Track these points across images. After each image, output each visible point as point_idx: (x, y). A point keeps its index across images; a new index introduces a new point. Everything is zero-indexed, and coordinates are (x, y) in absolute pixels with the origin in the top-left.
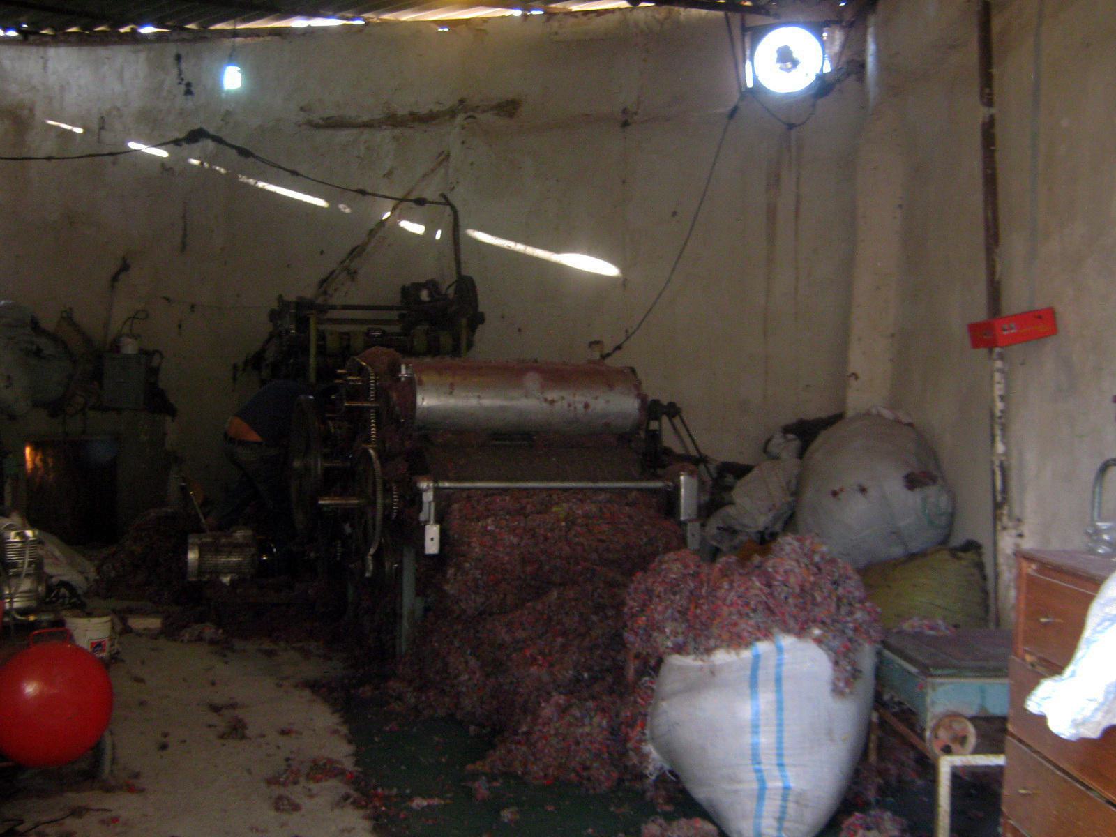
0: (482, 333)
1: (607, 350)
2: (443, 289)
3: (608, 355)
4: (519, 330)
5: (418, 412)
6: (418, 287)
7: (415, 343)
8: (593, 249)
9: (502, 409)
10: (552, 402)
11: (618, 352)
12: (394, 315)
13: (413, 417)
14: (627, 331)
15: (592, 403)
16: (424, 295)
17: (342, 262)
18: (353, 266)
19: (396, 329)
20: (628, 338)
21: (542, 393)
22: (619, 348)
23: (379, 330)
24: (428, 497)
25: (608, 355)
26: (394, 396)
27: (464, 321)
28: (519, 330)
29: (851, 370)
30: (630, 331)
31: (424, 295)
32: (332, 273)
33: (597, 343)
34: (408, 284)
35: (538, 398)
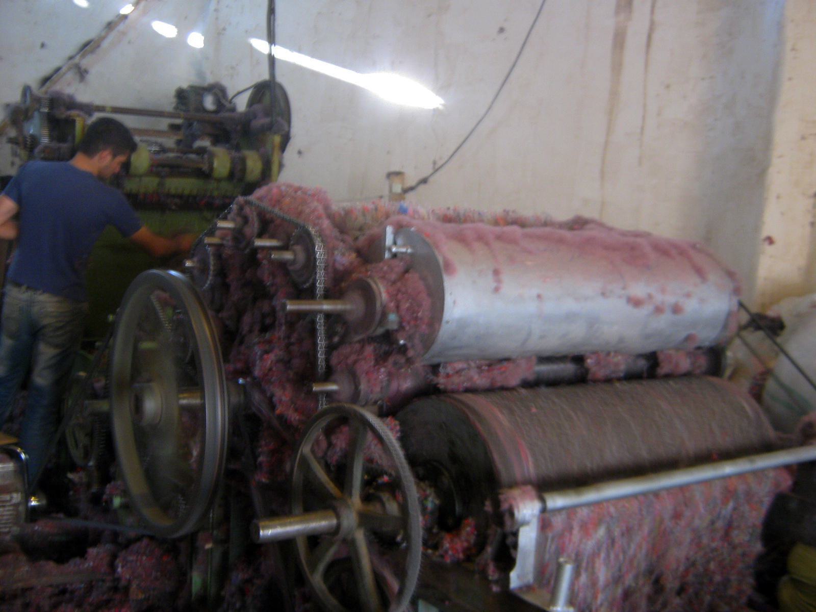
1: (411, 182)
2: (230, 93)
3: (412, 189)
4: (300, 153)
5: (445, 331)
6: (199, 91)
7: (216, 164)
8: (394, 66)
9: (570, 317)
10: (636, 303)
11: (422, 188)
12: (163, 124)
13: (428, 341)
14: (435, 163)
16: (209, 103)
17: (71, 58)
18: (85, 63)
20: (436, 171)
22: (424, 181)
23: (156, 143)
24: (527, 537)
25: (412, 189)
26: (382, 292)
27: (277, 139)
28: (300, 153)
30: (440, 163)
31: (209, 103)
32: (58, 70)
33: (398, 174)
34: (185, 86)
35: (620, 297)
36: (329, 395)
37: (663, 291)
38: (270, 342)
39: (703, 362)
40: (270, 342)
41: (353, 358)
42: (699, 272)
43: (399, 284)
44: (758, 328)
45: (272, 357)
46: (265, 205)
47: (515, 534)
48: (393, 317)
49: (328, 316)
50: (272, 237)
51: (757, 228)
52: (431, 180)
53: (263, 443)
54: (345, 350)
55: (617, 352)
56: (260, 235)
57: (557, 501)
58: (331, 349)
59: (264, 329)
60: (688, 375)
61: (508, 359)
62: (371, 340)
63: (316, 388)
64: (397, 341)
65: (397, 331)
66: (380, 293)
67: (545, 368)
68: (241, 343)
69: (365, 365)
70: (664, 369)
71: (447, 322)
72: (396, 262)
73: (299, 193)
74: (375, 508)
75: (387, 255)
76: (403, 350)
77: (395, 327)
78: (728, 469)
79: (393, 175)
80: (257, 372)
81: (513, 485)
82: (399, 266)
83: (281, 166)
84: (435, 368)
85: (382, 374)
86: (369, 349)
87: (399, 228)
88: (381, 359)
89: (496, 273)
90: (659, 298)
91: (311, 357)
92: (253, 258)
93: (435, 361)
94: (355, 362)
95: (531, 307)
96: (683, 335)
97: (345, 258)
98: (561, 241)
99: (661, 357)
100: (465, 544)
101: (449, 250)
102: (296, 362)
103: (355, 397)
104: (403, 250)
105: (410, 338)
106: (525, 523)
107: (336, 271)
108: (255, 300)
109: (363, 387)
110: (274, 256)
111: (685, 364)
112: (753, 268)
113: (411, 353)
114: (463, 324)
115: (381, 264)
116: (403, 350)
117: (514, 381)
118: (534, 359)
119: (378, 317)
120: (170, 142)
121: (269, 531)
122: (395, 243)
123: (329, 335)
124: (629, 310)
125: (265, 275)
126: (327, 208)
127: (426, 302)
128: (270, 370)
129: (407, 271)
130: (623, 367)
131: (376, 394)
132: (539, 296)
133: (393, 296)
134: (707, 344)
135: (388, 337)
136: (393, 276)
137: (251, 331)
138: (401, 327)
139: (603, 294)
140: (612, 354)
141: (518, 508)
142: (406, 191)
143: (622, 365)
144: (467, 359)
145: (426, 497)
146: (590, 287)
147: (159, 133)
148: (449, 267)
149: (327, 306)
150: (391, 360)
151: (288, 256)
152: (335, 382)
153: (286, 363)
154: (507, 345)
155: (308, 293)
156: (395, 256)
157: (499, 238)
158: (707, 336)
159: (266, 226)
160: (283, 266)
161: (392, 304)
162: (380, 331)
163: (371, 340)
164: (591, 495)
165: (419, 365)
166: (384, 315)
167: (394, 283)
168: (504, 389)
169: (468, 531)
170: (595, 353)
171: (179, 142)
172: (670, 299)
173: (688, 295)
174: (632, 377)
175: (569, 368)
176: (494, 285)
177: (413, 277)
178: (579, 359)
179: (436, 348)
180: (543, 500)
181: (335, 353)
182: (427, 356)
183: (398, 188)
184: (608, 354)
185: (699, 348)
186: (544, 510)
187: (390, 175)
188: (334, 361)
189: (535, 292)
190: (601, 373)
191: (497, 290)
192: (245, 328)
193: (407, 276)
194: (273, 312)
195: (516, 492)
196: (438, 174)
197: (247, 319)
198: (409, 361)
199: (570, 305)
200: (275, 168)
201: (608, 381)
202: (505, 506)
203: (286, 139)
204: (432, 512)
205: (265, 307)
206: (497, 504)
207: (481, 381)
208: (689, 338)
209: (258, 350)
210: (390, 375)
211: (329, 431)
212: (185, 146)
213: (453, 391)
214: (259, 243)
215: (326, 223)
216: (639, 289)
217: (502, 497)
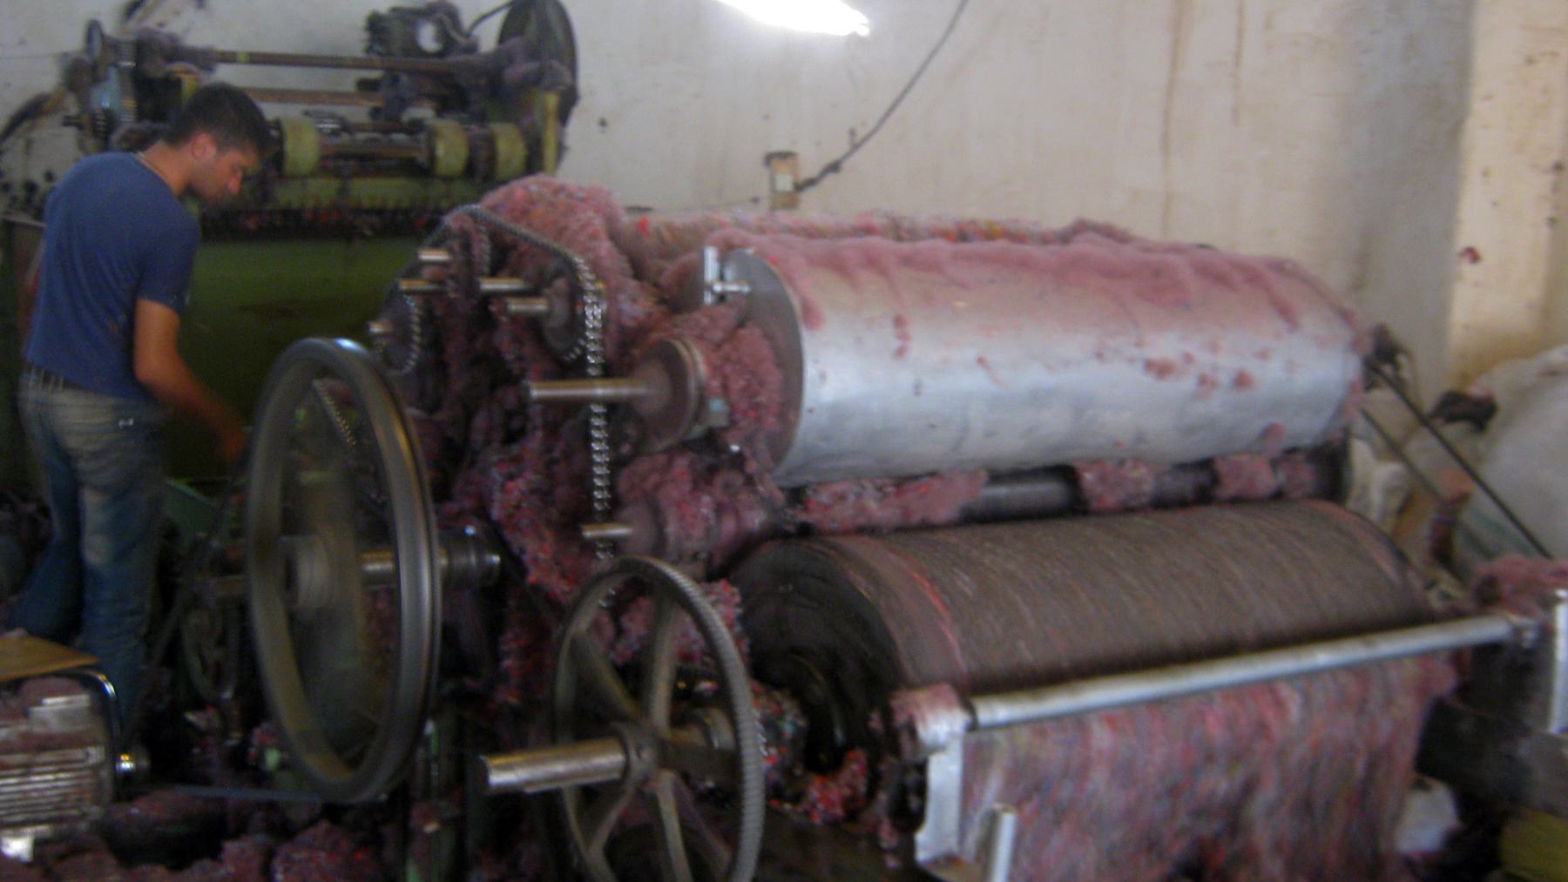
0: (579, 128)
1: (809, 169)
3: (811, 182)
4: (603, 123)
7: (441, 150)
9: (1038, 398)
10: (1161, 370)
11: (831, 179)
13: (780, 444)
14: (852, 133)
15: (1252, 367)
19: (358, 113)
20: (855, 147)
21: (1139, 344)
22: (834, 167)
23: (332, 116)
24: (944, 773)
25: (811, 182)
26: (698, 362)
27: (552, 100)
28: (603, 123)
29: (1464, 239)
30: (861, 134)
33: (785, 156)
35: (1131, 361)
36: (615, 545)
37: (1214, 348)
38: (517, 460)
39: (1307, 476)
40: (517, 460)
41: (654, 479)
42: (1286, 313)
43: (727, 348)
44: (1452, 419)
45: (520, 484)
46: (502, 219)
47: (922, 768)
48: (717, 405)
49: (614, 408)
50: (514, 274)
51: (1448, 235)
52: (847, 165)
53: (509, 635)
54: (642, 466)
55: (1138, 460)
56: (494, 273)
57: (995, 711)
58: (617, 465)
59: (512, 437)
60: (1278, 496)
61: (933, 474)
62: (685, 446)
63: (589, 533)
64: (726, 449)
65: (724, 429)
66: (695, 364)
67: (1001, 491)
68: (473, 463)
69: (676, 489)
70: (1229, 488)
71: (811, 411)
72: (722, 309)
73: (562, 197)
74: (693, 736)
75: (708, 299)
76: (738, 461)
77: (721, 422)
78: (1323, 657)
79: (774, 158)
80: (496, 513)
81: (927, 682)
82: (729, 315)
83: (561, 149)
84: (797, 495)
85: (706, 505)
86: (682, 463)
87: (728, 251)
88: (704, 479)
89: (899, 322)
90: (1204, 358)
91: (583, 481)
92: (484, 311)
93: (799, 480)
94: (657, 487)
95: (972, 382)
96: (1258, 425)
97: (636, 306)
98: (1024, 264)
99: (1222, 467)
100: (847, 792)
101: (813, 286)
102: (563, 492)
103: (659, 547)
104: (733, 288)
105: (748, 440)
106: (938, 748)
107: (622, 329)
108: (493, 386)
109: (671, 529)
110: (515, 306)
111: (1266, 481)
112: (1442, 309)
113: (752, 466)
114: (839, 413)
115: (697, 315)
116: (738, 461)
117: (943, 513)
118: (983, 476)
119: (692, 405)
120: (358, 113)
121: (505, 774)
122: (722, 278)
123: (613, 442)
124: (1148, 380)
125: (503, 340)
126: (610, 220)
127: (774, 377)
128: (518, 507)
129: (741, 324)
130: (1148, 487)
131: (696, 540)
132: (981, 361)
133: (715, 369)
134: (1307, 441)
135: (712, 440)
136: (718, 335)
137: (488, 442)
138: (733, 423)
139: (1099, 356)
140: (1129, 464)
141: (924, 720)
142: (800, 187)
143: (1145, 482)
144: (857, 476)
145: (781, 714)
146: (1074, 345)
147: (338, 97)
148: (812, 316)
149: (602, 390)
150: (719, 480)
151: (540, 306)
152: (625, 523)
153: (544, 494)
154: (927, 450)
155: (574, 369)
156: (721, 298)
157: (907, 261)
158: (1306, 428)
159: (504, 256)
160: (533, 325)
161: (715, 384)
162: (698, 430)
163: (685, 446)
164: (1058, 702)
165: (770, 487)
166: (702, 401)
167: (718, 346)
168: (927, 527)
169: (854, 768)
170: (1096, 462)
171: (375, 112)
172: (1226, 363)
173: (1263, 355)
174: (1162, 503)
175: (1049, 491)
176: (895, 344)
177: (750, 333)
178: (1065, 473)
179: (794, 456)
180: (969, 708)
181: (625, 474)
182: (781, 470)
183: (785, 183)
184: (1122, 463)
185: (1292, 451)
186: (973, 727)
187: (771, 159)
188: (623, 486)
189: (971, 354)
190: (1111, 500)
191: (900, 353)
192: (477, 437)
193: (743, 332)
194: (524, 403)
195: (921, 696)
196: (857, 157)
197: (480, 421)
198: (750, 481)
199: (1035, 376)
200: (550, 151)
201: (1127, 510)
202: (900, 719)
203: (569, 99)
204: (794, 741)
205: (509, 398)
206: (888, 715)
207: (878, 510)
208: (1269, 432)
209: (496, 474)
210: (720, 509)
211: (618, 609)
212: (387, 118)
213: (833, 533)
214: (488, 285)
215: (605, 247)
216: (1166, 345)
217: (895, 703)
